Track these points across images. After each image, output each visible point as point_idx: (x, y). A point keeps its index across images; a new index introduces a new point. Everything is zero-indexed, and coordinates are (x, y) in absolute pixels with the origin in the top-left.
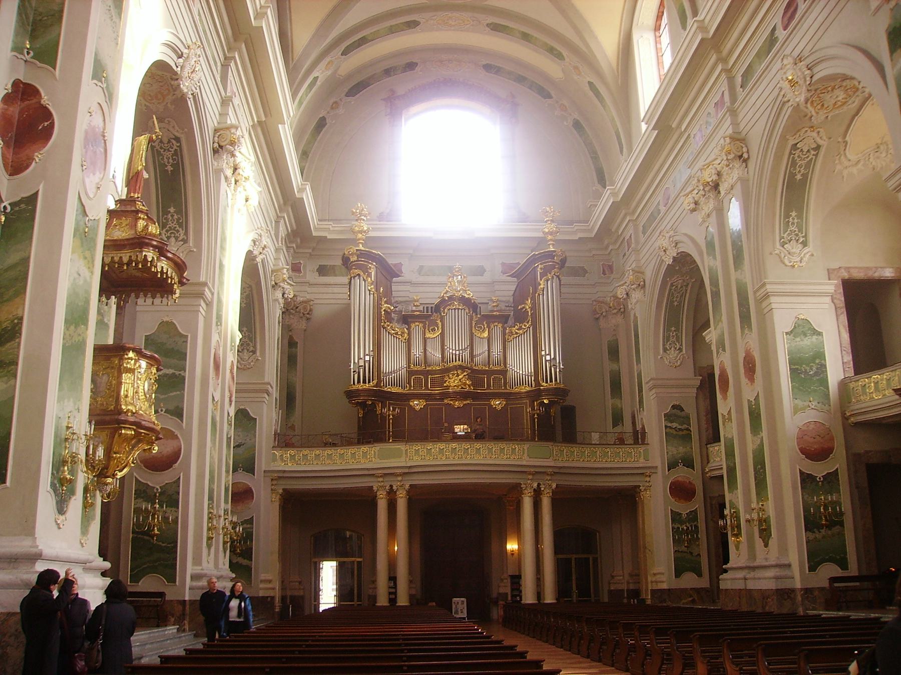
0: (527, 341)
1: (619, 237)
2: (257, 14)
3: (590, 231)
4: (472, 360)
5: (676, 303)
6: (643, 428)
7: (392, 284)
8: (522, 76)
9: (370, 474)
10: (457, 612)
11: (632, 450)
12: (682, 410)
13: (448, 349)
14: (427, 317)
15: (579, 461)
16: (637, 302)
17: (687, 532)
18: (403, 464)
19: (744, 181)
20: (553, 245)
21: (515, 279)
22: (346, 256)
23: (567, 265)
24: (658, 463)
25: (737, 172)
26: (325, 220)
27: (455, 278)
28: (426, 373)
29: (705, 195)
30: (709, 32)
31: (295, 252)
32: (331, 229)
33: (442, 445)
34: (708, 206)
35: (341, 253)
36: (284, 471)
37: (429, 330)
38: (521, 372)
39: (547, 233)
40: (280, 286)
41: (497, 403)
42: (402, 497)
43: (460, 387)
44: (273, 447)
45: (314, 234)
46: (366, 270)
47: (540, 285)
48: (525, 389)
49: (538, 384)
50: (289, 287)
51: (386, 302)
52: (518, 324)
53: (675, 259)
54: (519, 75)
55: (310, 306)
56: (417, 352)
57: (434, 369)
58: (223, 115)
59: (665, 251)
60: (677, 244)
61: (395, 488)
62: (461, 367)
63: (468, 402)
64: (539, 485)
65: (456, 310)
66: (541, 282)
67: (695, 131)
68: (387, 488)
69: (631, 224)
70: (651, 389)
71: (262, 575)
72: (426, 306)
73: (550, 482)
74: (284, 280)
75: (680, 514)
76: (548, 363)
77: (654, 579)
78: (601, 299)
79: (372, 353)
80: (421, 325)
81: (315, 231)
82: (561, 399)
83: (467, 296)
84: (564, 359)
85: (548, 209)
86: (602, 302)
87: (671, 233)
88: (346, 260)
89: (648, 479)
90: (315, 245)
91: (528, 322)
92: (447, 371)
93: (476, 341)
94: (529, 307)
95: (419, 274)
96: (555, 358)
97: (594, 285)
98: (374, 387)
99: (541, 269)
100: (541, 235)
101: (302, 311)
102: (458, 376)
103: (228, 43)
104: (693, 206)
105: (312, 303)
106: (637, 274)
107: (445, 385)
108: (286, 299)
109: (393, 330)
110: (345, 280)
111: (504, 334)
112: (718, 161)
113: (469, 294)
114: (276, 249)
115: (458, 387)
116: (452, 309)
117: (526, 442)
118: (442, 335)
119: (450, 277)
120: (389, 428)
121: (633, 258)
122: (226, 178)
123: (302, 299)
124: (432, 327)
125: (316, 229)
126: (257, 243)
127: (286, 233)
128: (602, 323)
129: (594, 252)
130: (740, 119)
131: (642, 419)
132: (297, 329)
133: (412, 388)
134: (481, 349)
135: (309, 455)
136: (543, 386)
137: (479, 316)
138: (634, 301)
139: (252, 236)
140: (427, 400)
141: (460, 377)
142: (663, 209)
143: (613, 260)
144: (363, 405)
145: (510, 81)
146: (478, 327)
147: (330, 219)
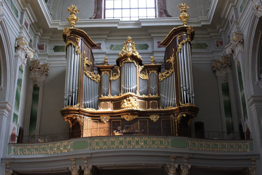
6: (248, 130)
9: (66, 159)
11: (242, 144)
14: (112, 68)
15: (206, 150)
16: (239, 52)
31: (41, 39)
32: (60, 24)
36: (14, 159)
40: (21, 48)
45: (50, 27)
47: (178, 47)
50: (30, 52)
52: (166, 71)
59: (257, 8)
61: (83, 168)
64: (179, 166)
65: (129, 63)
66: (180, 45)
69: (233, 8)
70: (252, 104)
78: (216, 60)
81: (51, 25)
82: (194, 114)
83: (135, 54)
84: (195, 90)
86: (217, 62)
89: (253, 163)
91: (172, 69)
95: (111, 49)
96: (189, 89)
97: (212, 53)
99: (179, 38)
101: (43, 70)
106: (238, 35)
109: (91, 75)
114: (20, 27)
116: (126, 63)
117: (169, 137)
118: (120, 77)
123: (42, 63)
125: (52, 24)
127: (31, 23)
128: (218, 73)
129: (211, 34)
131: (247, 124)
136: (181, 106)
143: (223, 37)
146: (142, 73)
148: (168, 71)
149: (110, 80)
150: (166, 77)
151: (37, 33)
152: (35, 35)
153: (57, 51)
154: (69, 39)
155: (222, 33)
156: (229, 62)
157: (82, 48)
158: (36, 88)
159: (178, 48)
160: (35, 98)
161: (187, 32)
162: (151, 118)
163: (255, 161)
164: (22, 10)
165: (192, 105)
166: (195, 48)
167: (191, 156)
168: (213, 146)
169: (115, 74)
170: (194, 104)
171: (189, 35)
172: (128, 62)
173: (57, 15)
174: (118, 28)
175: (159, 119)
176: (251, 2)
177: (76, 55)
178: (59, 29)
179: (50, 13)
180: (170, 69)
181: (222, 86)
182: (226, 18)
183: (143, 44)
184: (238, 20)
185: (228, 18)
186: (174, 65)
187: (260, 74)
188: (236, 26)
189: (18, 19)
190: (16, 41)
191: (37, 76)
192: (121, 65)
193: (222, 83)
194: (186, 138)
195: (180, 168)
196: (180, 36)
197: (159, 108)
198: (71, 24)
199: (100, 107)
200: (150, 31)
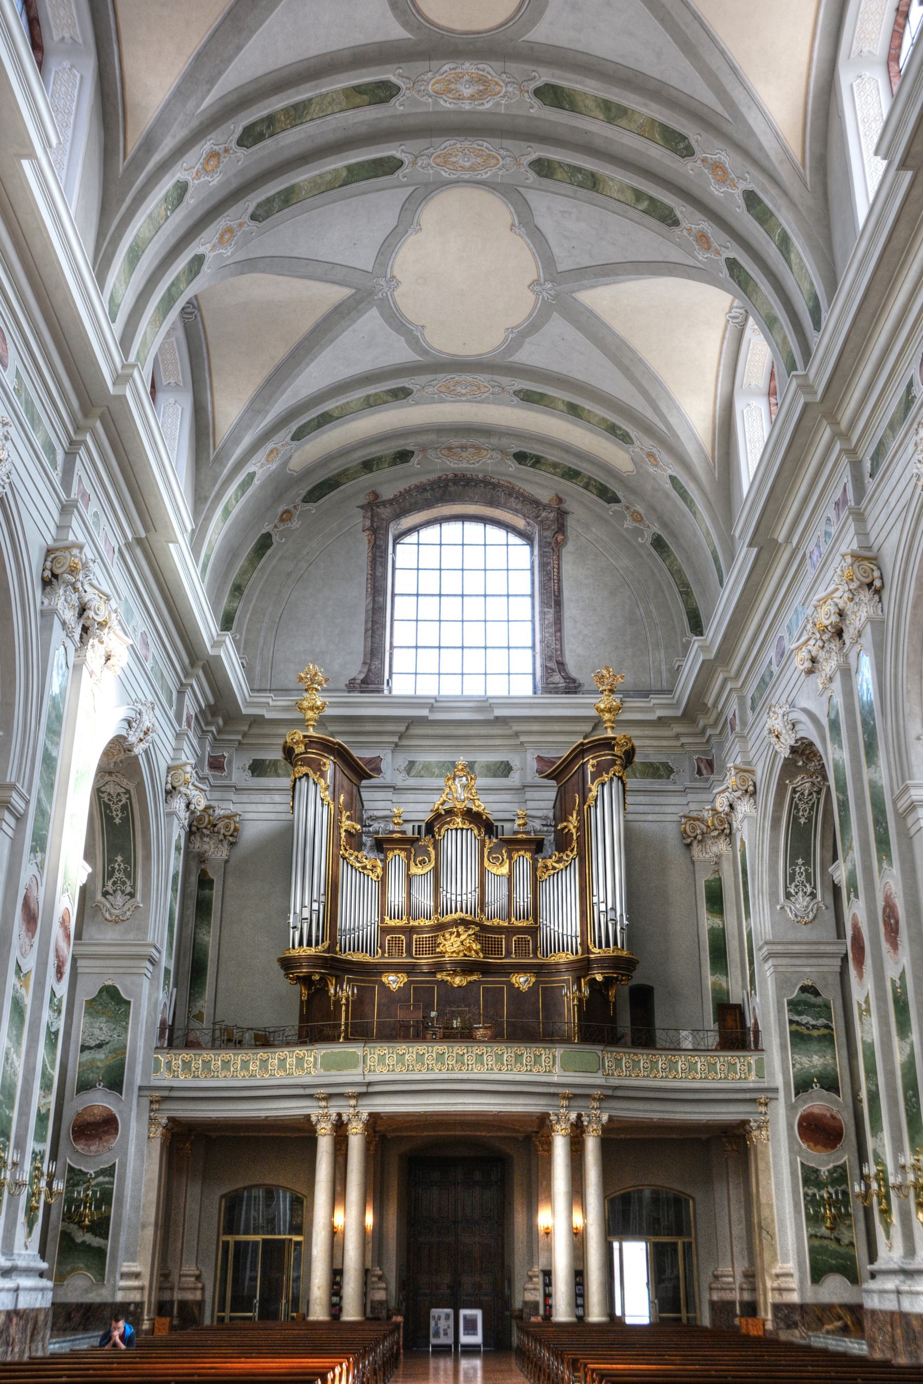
0: (570, 882)
1: (720, 714)
2: (118, 376)
3: (676, 706)
4: (482, 910)
5: (802, 821)
6: (756, 1023)
7: (361, 790)
8: (574, 470)
10: (437, 1335)
11: (737, 1061)
12: (817, 993)
13: (445, 893)
14: (413, 841)
16: (745, 817)
17: (831, 1203)
18: (359, 1079)
19: (878, 626)
20: (613, 728)
21: (554, 782)
22: (288, 745)
23: (637, 759)
24: (779, 1082)
25: (865, 610)
26: (265, 690)
27: (457, 780)
28: (409, 931)
29: (823, 647)
30: (816, 393)
31: (215, 739)
32: (271, 703)
33: (421, 1048)
34: (830, 665)
35: (281, 741)
36: (171, 1089)
37: (415, 861)
38: (560, 931)
39: (602, 711)
40: (180, 792)
41: (522, 980)
42: (356, 1134)
43: (461, 954)
44: (157, 1048)
45: (245, 711)
46: (318, 768)
48: (563, 958)
49: (587, 950)
50: (197, 792)
51: (348, 818)
52: (557, 853)
53: (793, 750)
54: (570, 468)
55: (235, 822)
56: (396, 896)
57: (422, 924)
58: (63, 527)
60: (794, 725)
61: (345, 1118)
62: (464, 922)
63: (474, 978)
64: (579, 1116)
65: (459, 831)
66: (594, 788)
67: (812, 546)
68: (334, 1117)
69: (734, 695)
70: (766, 959)
71: (125, 1264)
72: (417, 824)
73: (598, 1112)
74: (186, 783)
75: (817, 1170)
76: (602, 916)
77: (775, 1285)
78: (694, 814)
79: (322, 899)
80: (403, 854)
81: (246, 707)
82: (623, 975)
83: (475, 809)
85: (604, 672)
86: (695, 819)
87: (786, 708)
88: (288, 752)
90: (246, 728)
91: (572, 851)
92: (441, 927)
93: (489, 879)
94: (574, 827)
95: (408, 774)
96: (614, 909)
98: (324, 952)
99: (593, 766)
100: (594, 713)
101: (222, 831)
102: (459, 935)
103: (73, 419)
104: (808, 664)
105: (237, 819)
106: (742, 774)
107: (438, 950)
108: (193, 813)
109: (359, 862)
110: (286, 782)
111: (535, 869)
112: (838, 594)
113: (479, 806)
114: (177, 734)
115: (458, 953)
117: (557, 1045)
118: (436, 871)
119: (449, 779)
121: (737, 749)
122: (64, 624)
123: (222, 812)
124: (421, 858)
125: (248, 704)
126: (134, 724)
127: (197, 710)
128: (696, 849)
129: (684, 740)
130: (869, 525)
131: (754, 1009)
132: (214, 859)
133: (386, 955)
134: (496, 896)
135: (213, 1062)
136: (594, 953)
137: (495, 840)
138: (740, 816)
139: (123, 712)
140: (409, 974)
141: (463, 937)
142: (775, 669)
143: (714, 751)
144: (306, 981)
145: (556, 478)
146: (493, 858)
147: (273, 688)
151: (209, 728)
152: (203, 731)
153: (258, 776)
154: (301, 760)
155: (713, 740)
156: (726, 826)
157: (337, 789)
158: (205, 882)
159: (590, 795)
160: (203, 909)
161: (614, 750)
162: (513, 980)
163: (766, 1104)
164: (182, 684)
165: (620, 953)
166: (638, 775)
167: (609, 1093)
168: (664, 1066)
170: (628, 949)
171: (620, 757)
172: (456, 829)
173: (258, 668)
176: (766, 715)
178: (268, 715)
179: (242, 664)
181: (706, 886)
182: (720, 707)
183: (496, 763)
184: (746, 732)
185: (725, 713)
186: (577, 838)
188: (740, 747)
189: (171, 714)
190: (168, 773)
191: (206, 847)
192: (440, 835)
194: (598, 1049)
195: (582, 1122)
196: (595, 761)
197: (536, 956)
198: (308, 720)
200: (516, 727)
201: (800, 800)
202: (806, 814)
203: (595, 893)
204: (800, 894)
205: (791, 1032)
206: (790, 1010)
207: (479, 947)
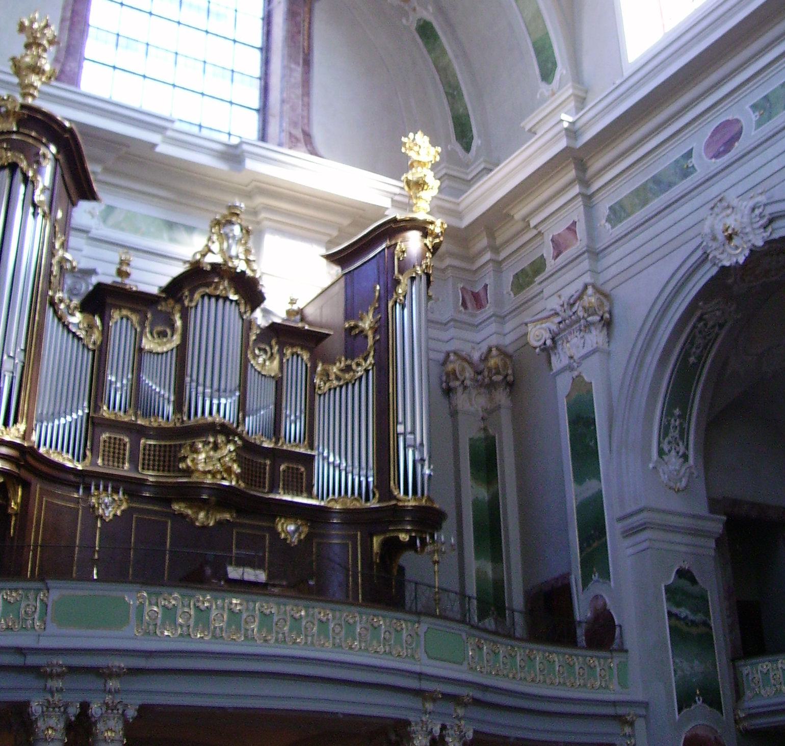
5: (692, 359)
11: (597, 663)
12: (693, 581)
13: (194, 384)
41: (291, 528)
63: (227, 516)
64: (444, 727)
68: (74, 711)
80: (135, 318)
86: (464, 359)
89: (627, 730)
91: (365, 359)
97: (446, 324)
102: (216, 447)
107: (182, 466)
118: (182, 349)
120: (35, 556)
148: (349, 362)
149: (141, 350)
150: (341, 383)
156: (510, 372)
169: (159, 328)
174: (159, 149)
175: (307, 536)
177: (30, 217)
180: (358, 356)
181: (471, 446)
186: (375, 342)
187: (664, 439)
193: (471, 436)
199: (92, 450)
201: (700, 332)
202: (698, 351)
203: (400, 419)
204: (673, 453)
205: (670, 628)
206: (668, 599)
207: (239, 471)
